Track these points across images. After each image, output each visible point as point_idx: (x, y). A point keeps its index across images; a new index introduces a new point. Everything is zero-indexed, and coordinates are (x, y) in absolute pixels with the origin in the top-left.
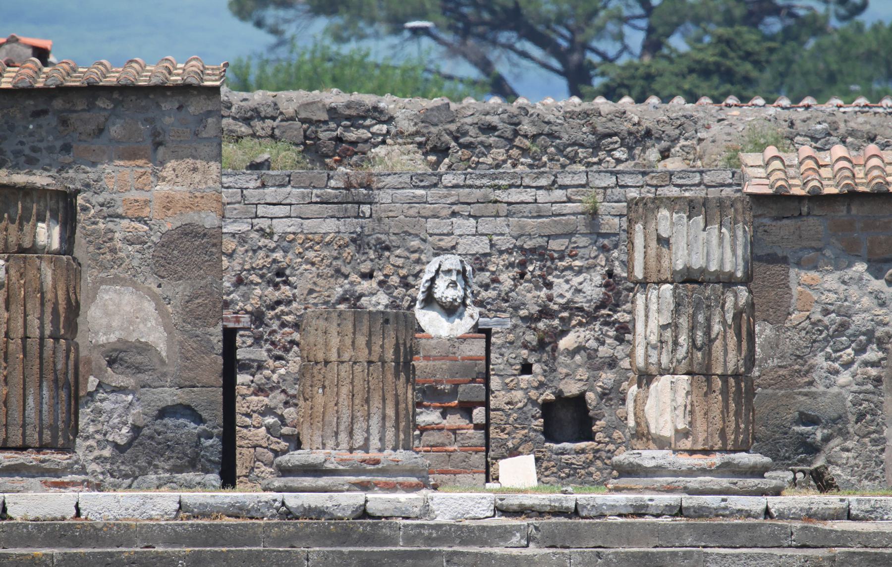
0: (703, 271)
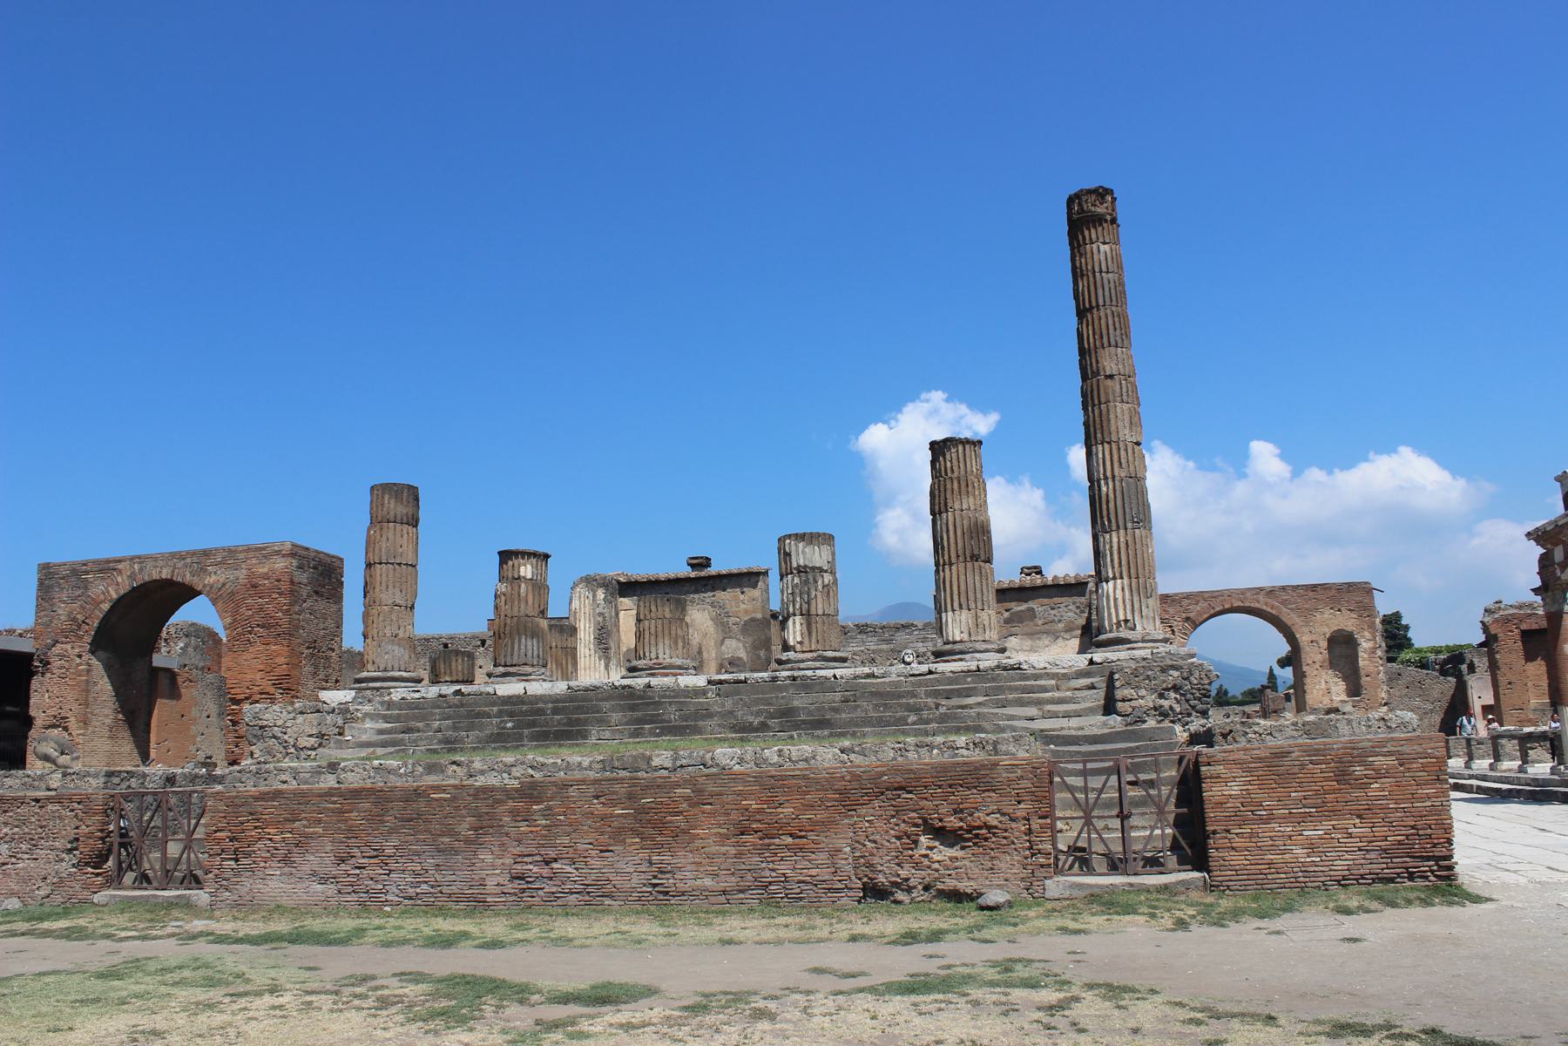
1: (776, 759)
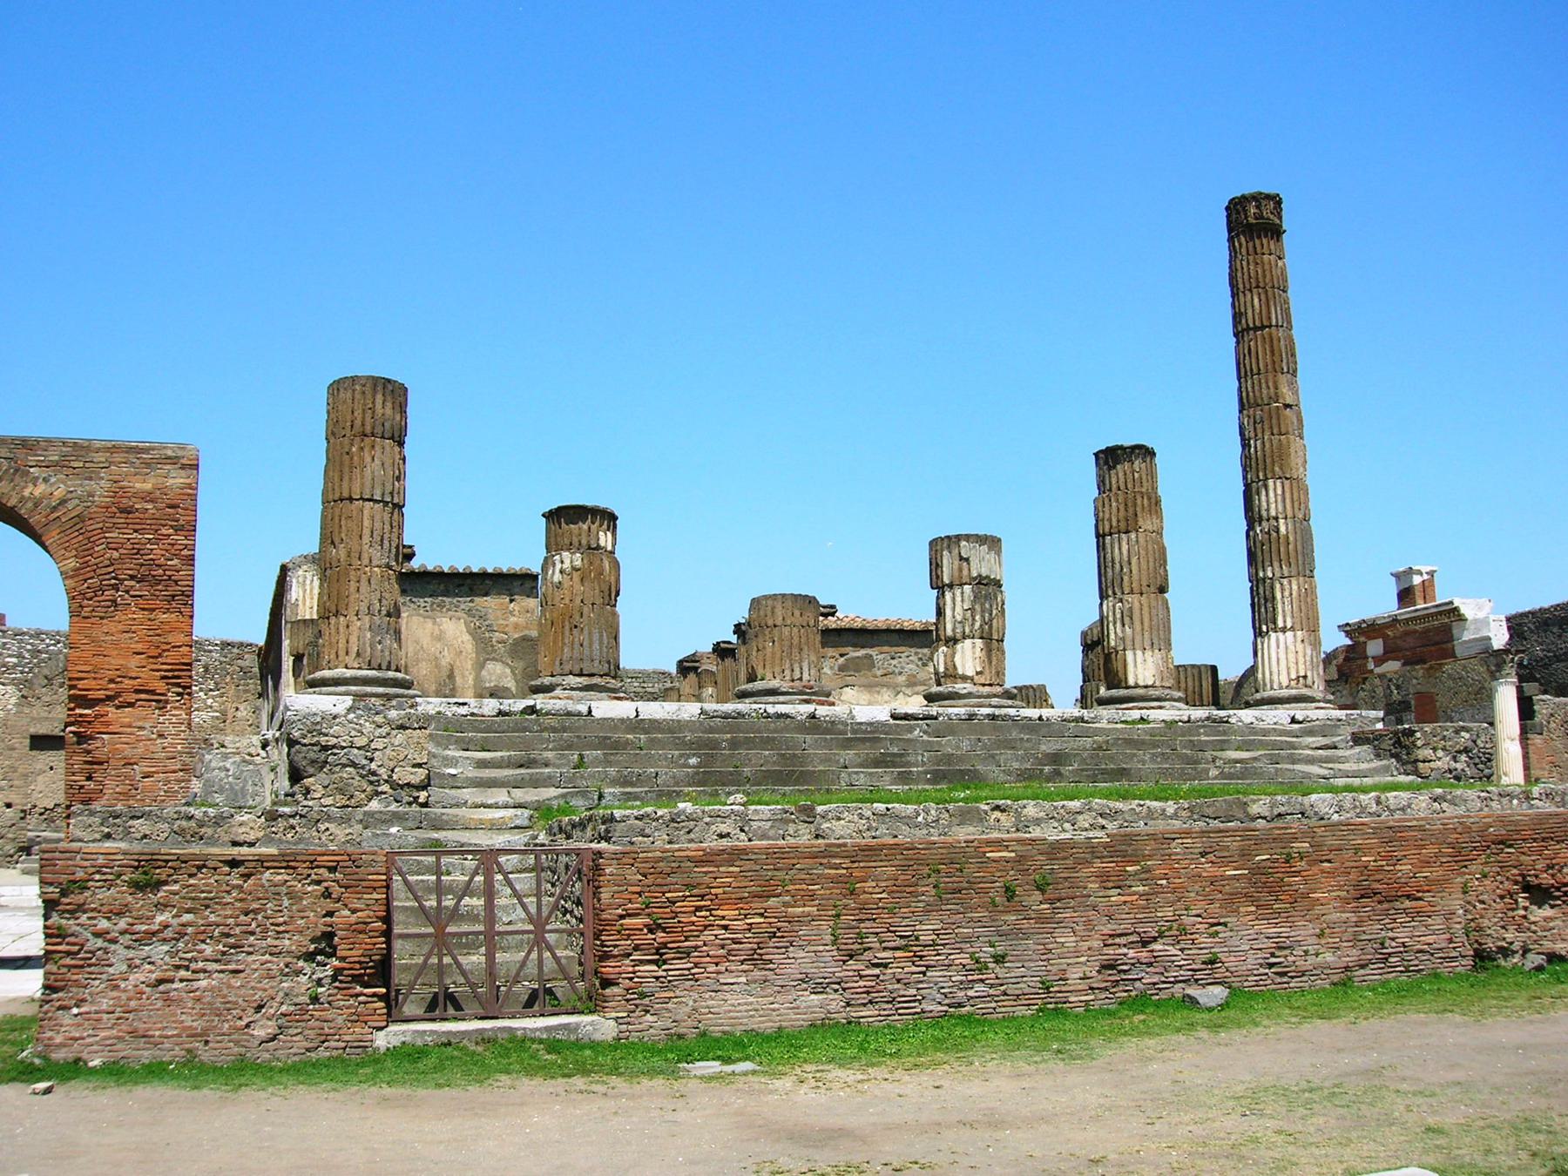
0: (987, 577)
1: (1374, 808)
